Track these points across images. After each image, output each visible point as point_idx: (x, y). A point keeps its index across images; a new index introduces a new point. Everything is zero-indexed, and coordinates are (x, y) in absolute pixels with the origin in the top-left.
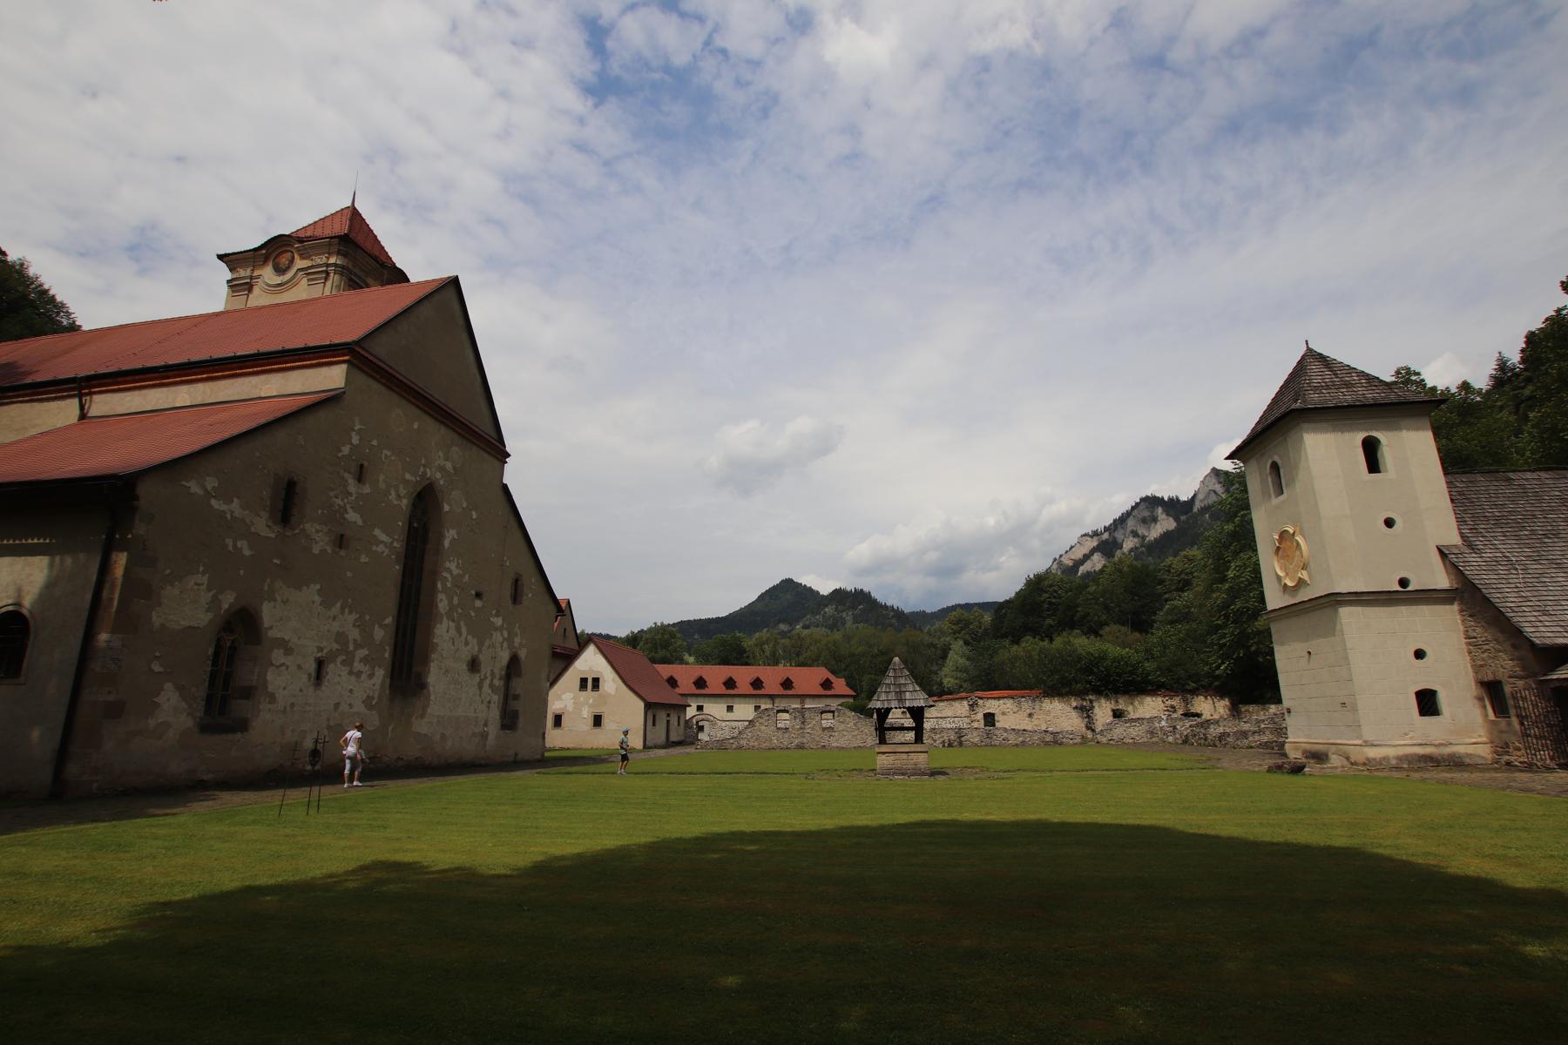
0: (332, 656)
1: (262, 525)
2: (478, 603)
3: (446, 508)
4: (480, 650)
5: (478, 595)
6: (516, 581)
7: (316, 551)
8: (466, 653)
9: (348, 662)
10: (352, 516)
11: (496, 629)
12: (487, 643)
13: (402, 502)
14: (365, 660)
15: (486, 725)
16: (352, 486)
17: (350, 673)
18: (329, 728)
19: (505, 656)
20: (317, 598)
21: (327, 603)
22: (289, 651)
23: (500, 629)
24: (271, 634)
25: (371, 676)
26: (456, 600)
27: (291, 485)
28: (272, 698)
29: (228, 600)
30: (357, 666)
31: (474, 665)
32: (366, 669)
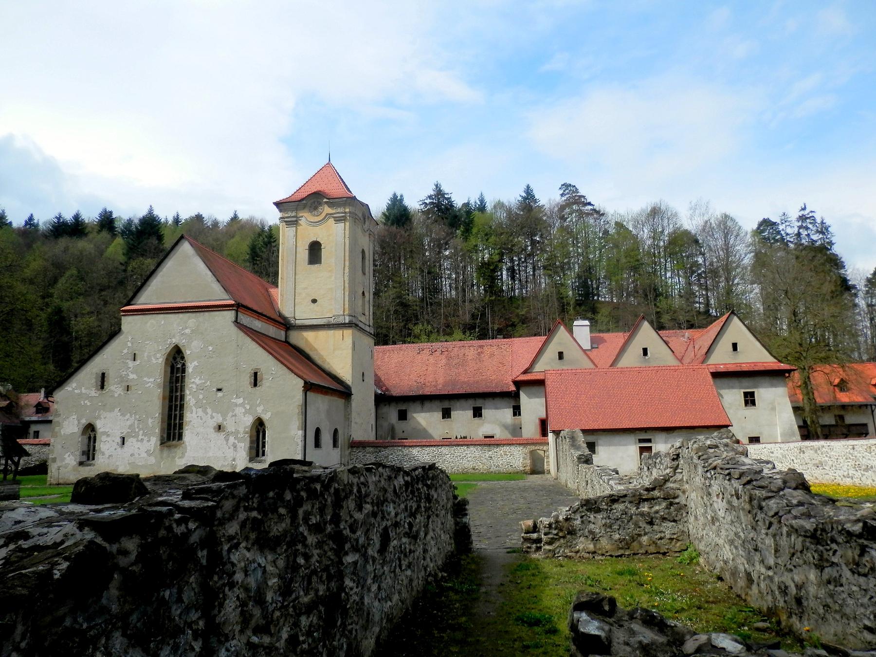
0: (130, 435)
1: (94, 392)
2: (220, 394)
3: (188, 352)
4: (224, 419)
5: (219, 390)
6: (256, 374)
7: (116, 395)
8: (213, 423)
9: (136, 436)
10: (132, 376)
11: (236, 405)
12: (230, 414)
13: (158, 361)
14: (144, 434)
15: (234, 460)
16: (131, 364)
17: (138, 441)
18: (129, 464)
19: (249, 420)
20: (119, 414)
21: (123, 415)
22: (108, 436)
23: (242, 405)
24: (101, 430)
25: (149, 441)
26: (201, 397)
27: (103, 374)
28: (103, 454)
29: (84, 422)
30: (140, 437)
31: (219, 428)
32: (146, 438)
